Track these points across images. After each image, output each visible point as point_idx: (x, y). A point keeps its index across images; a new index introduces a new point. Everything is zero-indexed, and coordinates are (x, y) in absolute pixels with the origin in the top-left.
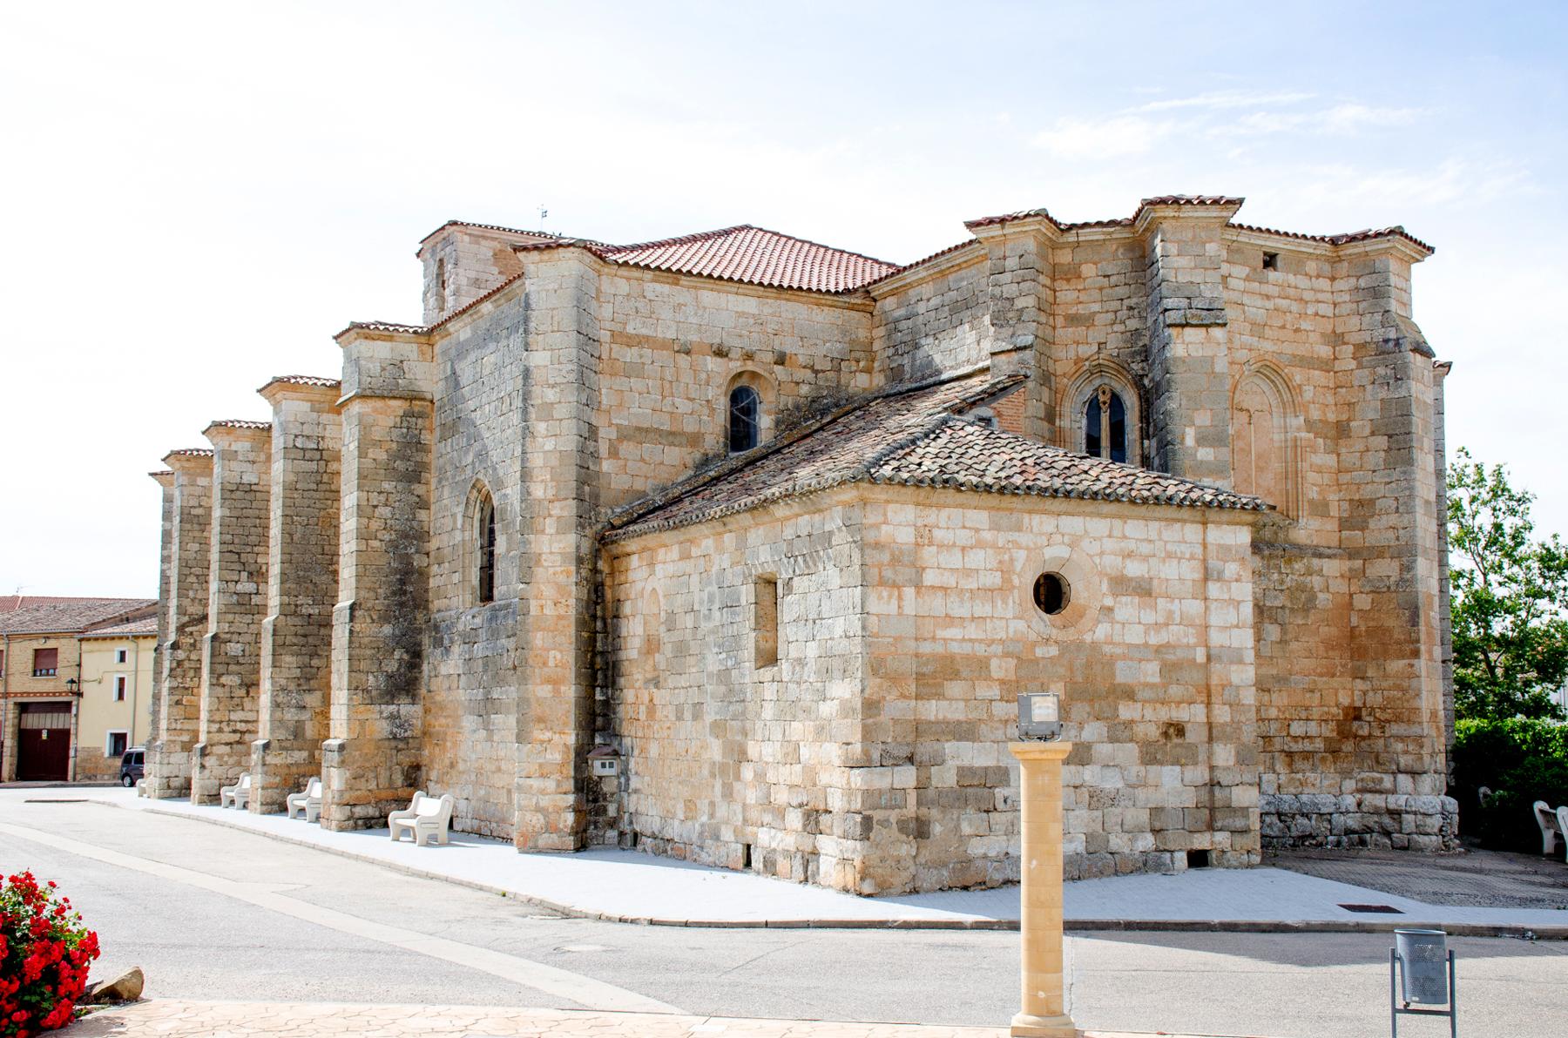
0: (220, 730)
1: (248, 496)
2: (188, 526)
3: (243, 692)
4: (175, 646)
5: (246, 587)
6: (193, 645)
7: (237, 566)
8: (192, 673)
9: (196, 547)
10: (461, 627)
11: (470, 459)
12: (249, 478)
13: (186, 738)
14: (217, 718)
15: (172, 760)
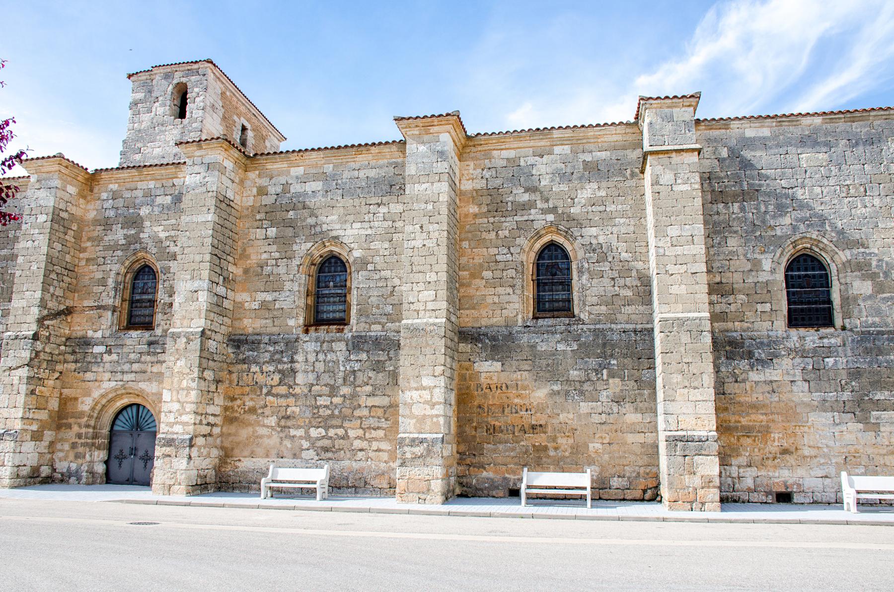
0: (201, 423)
1: (228, 209)
2: (56, 226)
3: (213, 388)
4: (36, 337)
5: (221, 290)
6: (48, 338)
7: (218, 270)
8: (44, 365)
9: (58, 247)
10: (790, 344)
11: (787, 220)
12: (230, 195)
13: (35, 427)
14: (200, 410)
15: (23, 449)
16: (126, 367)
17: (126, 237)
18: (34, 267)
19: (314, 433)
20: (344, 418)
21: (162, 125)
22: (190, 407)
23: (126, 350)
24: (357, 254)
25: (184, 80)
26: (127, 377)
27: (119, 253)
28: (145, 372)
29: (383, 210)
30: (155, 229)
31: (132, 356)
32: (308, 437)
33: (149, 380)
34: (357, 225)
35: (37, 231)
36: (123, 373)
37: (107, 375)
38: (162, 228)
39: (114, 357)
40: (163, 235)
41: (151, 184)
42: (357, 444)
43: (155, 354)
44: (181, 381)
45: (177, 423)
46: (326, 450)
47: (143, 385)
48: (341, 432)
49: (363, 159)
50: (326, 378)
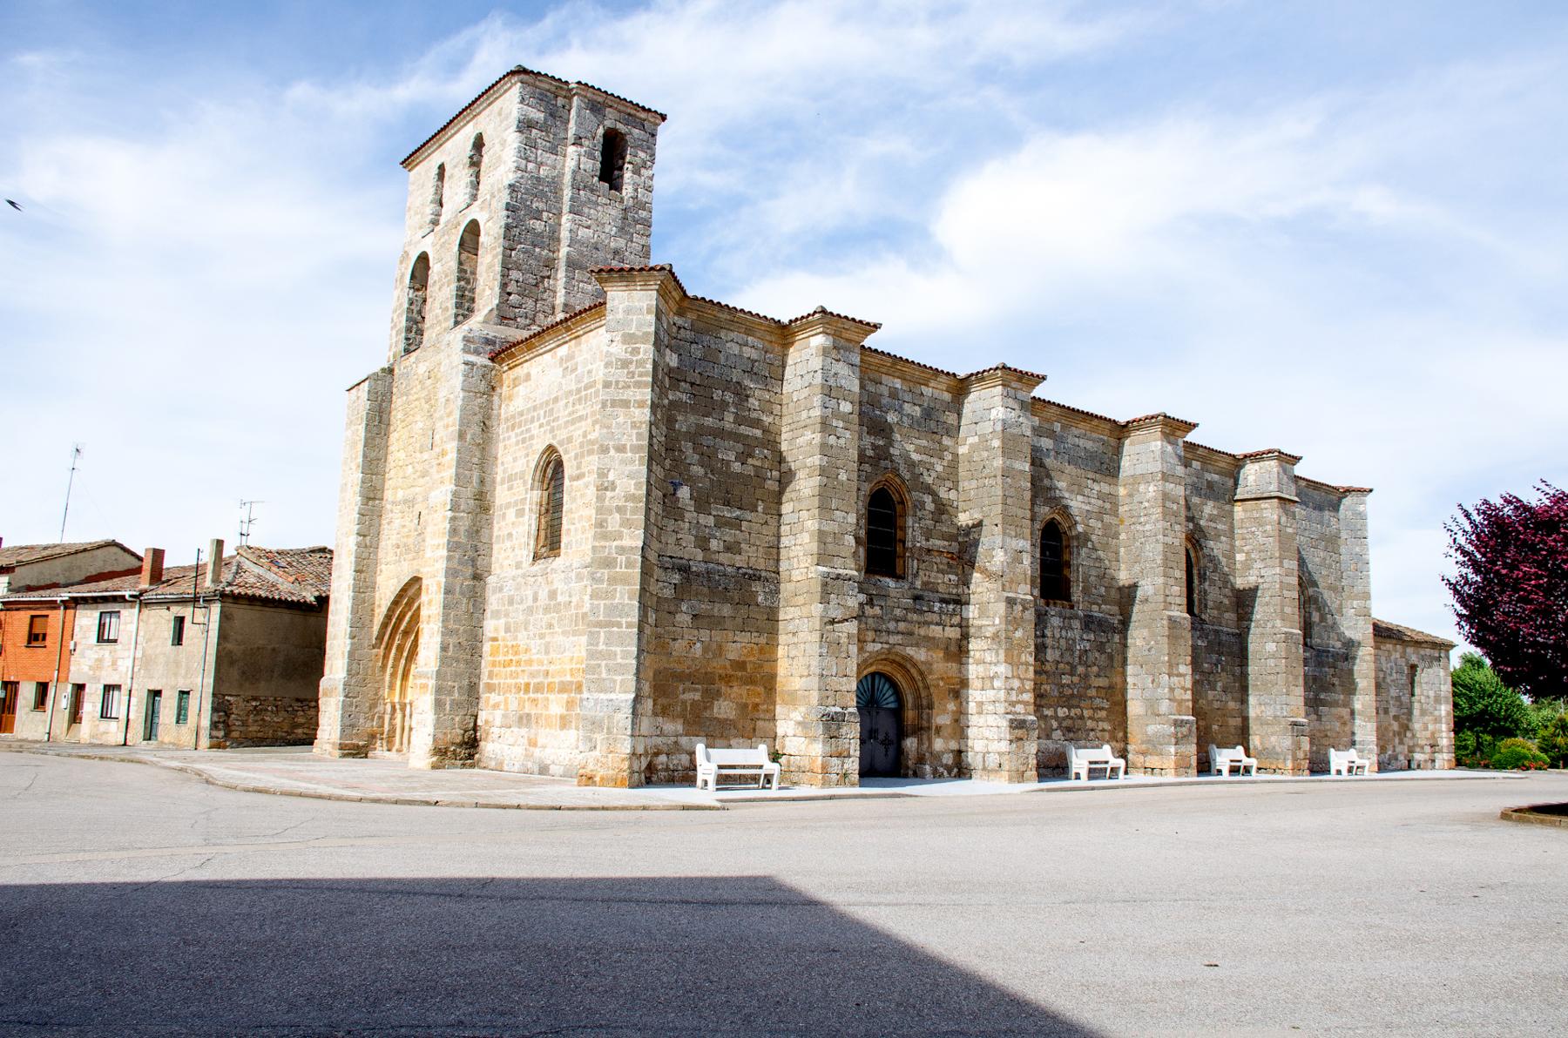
16: (892, 625)
17: (875, 447)
18: (843, 477)
19: (1062, 712)
20: (1081, 697)
21: (592, 191)
22: (1029, 685)
23: (890, 603)
24: (1080, 528)
25: (621, 127)
26: (893, 639)
27: (867, 467)
28: (911, 634)
29: (1096, 487)
30: (911, 448)
31: (898, 612)
32: (1056, 717)
33: (917, 645)
34: (1080, 498)
35: (841, 424)
36: (889, 632)
37: (870, 635)
38: (911, 448)
39: (877, 610)
40: (915, 457)
41: (898, 384)
42: (1090, 724)
43: (922, 612)
44: (1019, 656)
45: (1019, 702)
46: (1069, 730)
47: (910, 651)
48: (1078, 711)
49: (1083, 427)
50: (1067, 658)
